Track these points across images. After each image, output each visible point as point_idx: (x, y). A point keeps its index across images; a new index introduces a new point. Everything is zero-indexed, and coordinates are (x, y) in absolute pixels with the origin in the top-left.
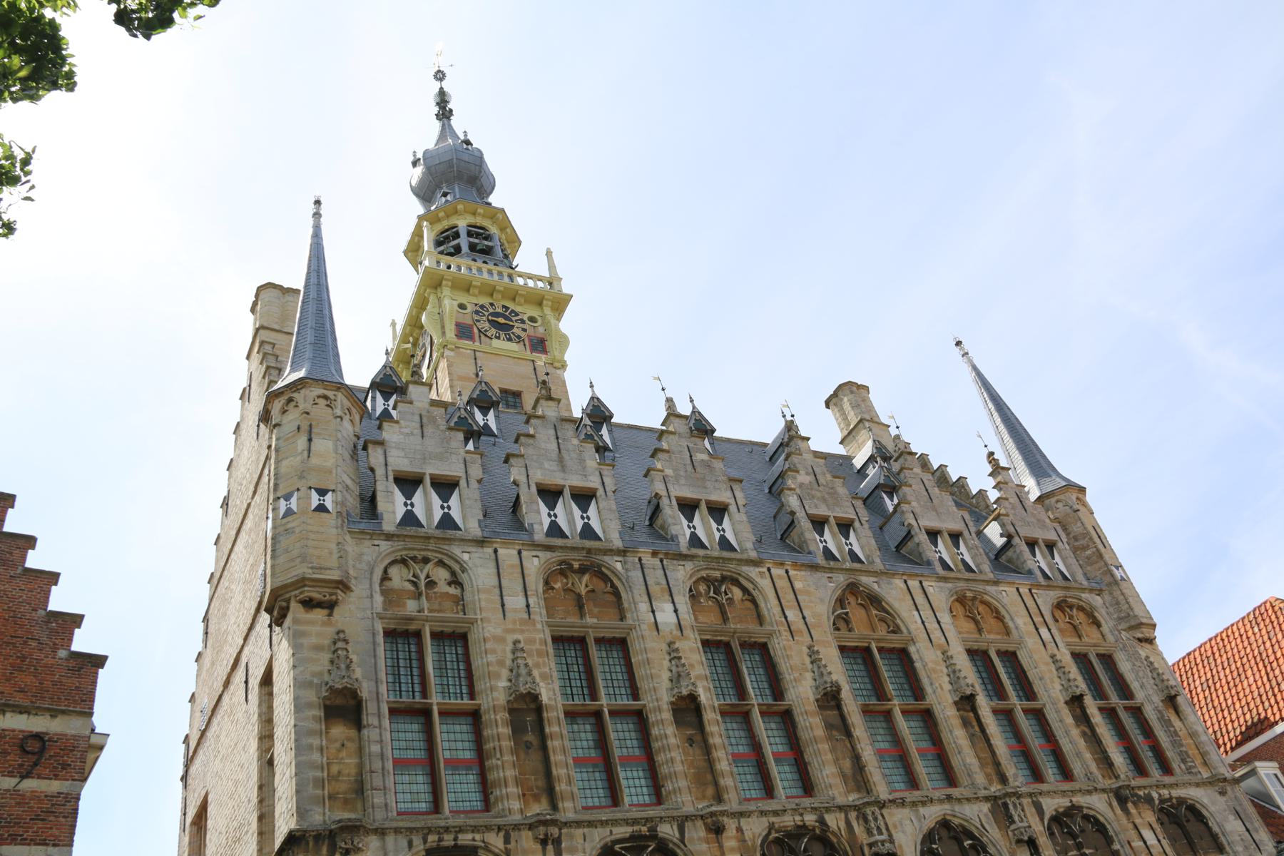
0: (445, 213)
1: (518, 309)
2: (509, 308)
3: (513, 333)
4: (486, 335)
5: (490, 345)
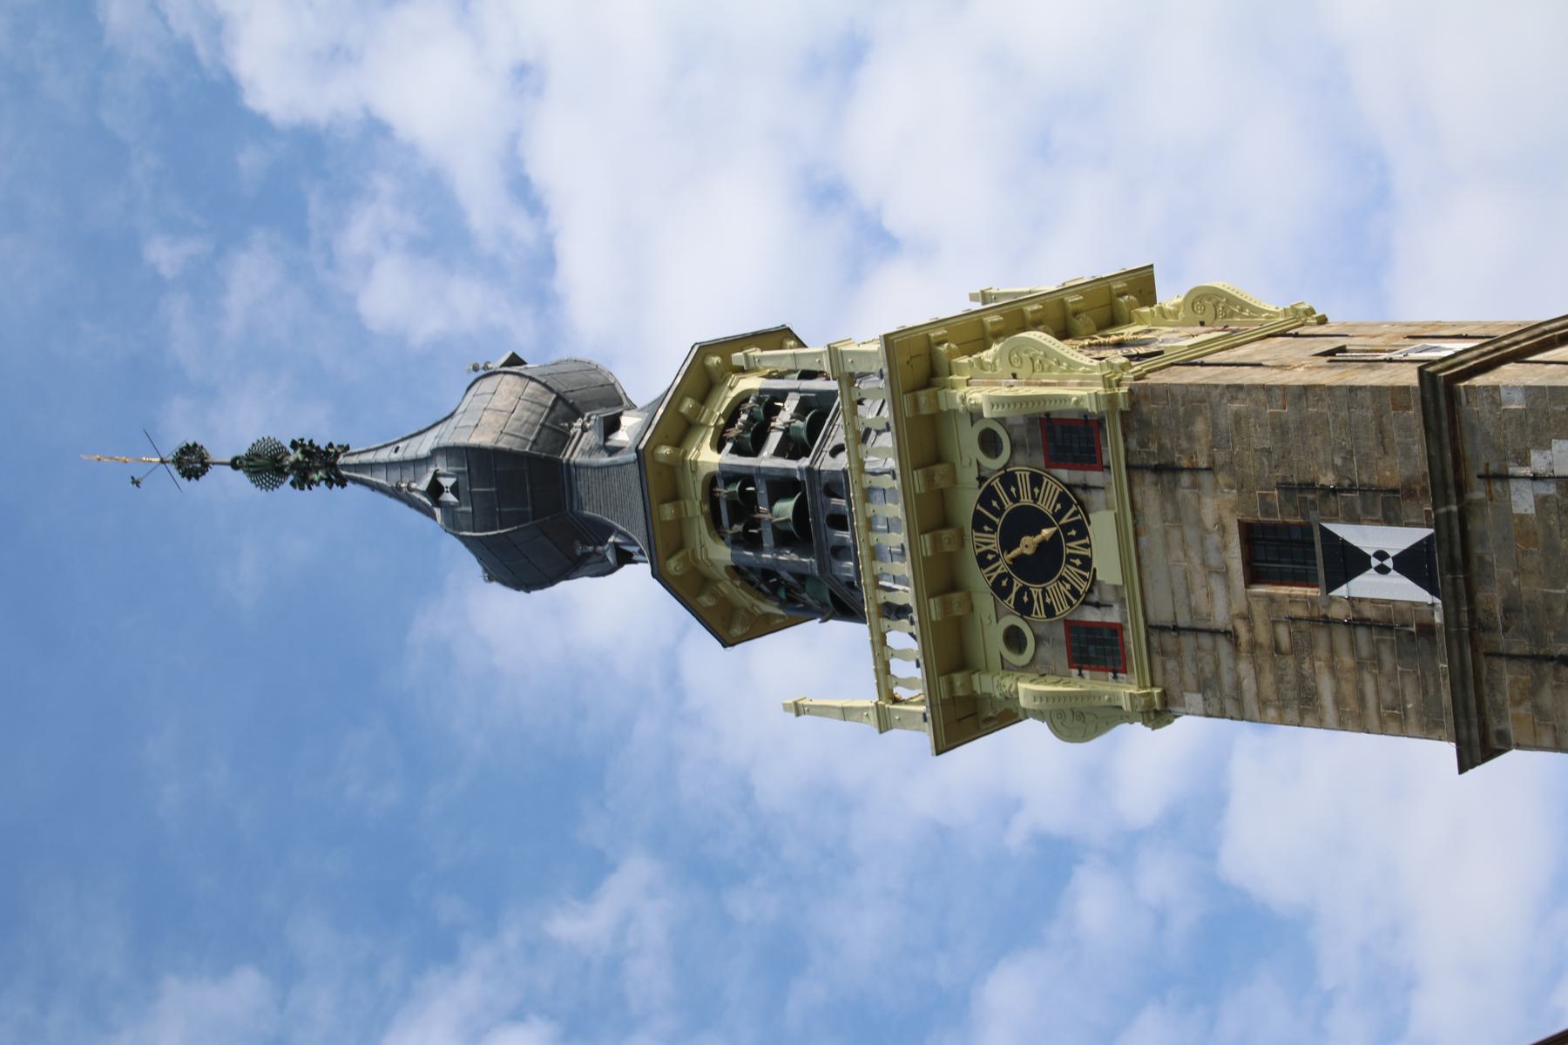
0: (699, 594)
1: (969, 476)
2: (977, 513)
4: (1090, 591)
5: (1116, 587)
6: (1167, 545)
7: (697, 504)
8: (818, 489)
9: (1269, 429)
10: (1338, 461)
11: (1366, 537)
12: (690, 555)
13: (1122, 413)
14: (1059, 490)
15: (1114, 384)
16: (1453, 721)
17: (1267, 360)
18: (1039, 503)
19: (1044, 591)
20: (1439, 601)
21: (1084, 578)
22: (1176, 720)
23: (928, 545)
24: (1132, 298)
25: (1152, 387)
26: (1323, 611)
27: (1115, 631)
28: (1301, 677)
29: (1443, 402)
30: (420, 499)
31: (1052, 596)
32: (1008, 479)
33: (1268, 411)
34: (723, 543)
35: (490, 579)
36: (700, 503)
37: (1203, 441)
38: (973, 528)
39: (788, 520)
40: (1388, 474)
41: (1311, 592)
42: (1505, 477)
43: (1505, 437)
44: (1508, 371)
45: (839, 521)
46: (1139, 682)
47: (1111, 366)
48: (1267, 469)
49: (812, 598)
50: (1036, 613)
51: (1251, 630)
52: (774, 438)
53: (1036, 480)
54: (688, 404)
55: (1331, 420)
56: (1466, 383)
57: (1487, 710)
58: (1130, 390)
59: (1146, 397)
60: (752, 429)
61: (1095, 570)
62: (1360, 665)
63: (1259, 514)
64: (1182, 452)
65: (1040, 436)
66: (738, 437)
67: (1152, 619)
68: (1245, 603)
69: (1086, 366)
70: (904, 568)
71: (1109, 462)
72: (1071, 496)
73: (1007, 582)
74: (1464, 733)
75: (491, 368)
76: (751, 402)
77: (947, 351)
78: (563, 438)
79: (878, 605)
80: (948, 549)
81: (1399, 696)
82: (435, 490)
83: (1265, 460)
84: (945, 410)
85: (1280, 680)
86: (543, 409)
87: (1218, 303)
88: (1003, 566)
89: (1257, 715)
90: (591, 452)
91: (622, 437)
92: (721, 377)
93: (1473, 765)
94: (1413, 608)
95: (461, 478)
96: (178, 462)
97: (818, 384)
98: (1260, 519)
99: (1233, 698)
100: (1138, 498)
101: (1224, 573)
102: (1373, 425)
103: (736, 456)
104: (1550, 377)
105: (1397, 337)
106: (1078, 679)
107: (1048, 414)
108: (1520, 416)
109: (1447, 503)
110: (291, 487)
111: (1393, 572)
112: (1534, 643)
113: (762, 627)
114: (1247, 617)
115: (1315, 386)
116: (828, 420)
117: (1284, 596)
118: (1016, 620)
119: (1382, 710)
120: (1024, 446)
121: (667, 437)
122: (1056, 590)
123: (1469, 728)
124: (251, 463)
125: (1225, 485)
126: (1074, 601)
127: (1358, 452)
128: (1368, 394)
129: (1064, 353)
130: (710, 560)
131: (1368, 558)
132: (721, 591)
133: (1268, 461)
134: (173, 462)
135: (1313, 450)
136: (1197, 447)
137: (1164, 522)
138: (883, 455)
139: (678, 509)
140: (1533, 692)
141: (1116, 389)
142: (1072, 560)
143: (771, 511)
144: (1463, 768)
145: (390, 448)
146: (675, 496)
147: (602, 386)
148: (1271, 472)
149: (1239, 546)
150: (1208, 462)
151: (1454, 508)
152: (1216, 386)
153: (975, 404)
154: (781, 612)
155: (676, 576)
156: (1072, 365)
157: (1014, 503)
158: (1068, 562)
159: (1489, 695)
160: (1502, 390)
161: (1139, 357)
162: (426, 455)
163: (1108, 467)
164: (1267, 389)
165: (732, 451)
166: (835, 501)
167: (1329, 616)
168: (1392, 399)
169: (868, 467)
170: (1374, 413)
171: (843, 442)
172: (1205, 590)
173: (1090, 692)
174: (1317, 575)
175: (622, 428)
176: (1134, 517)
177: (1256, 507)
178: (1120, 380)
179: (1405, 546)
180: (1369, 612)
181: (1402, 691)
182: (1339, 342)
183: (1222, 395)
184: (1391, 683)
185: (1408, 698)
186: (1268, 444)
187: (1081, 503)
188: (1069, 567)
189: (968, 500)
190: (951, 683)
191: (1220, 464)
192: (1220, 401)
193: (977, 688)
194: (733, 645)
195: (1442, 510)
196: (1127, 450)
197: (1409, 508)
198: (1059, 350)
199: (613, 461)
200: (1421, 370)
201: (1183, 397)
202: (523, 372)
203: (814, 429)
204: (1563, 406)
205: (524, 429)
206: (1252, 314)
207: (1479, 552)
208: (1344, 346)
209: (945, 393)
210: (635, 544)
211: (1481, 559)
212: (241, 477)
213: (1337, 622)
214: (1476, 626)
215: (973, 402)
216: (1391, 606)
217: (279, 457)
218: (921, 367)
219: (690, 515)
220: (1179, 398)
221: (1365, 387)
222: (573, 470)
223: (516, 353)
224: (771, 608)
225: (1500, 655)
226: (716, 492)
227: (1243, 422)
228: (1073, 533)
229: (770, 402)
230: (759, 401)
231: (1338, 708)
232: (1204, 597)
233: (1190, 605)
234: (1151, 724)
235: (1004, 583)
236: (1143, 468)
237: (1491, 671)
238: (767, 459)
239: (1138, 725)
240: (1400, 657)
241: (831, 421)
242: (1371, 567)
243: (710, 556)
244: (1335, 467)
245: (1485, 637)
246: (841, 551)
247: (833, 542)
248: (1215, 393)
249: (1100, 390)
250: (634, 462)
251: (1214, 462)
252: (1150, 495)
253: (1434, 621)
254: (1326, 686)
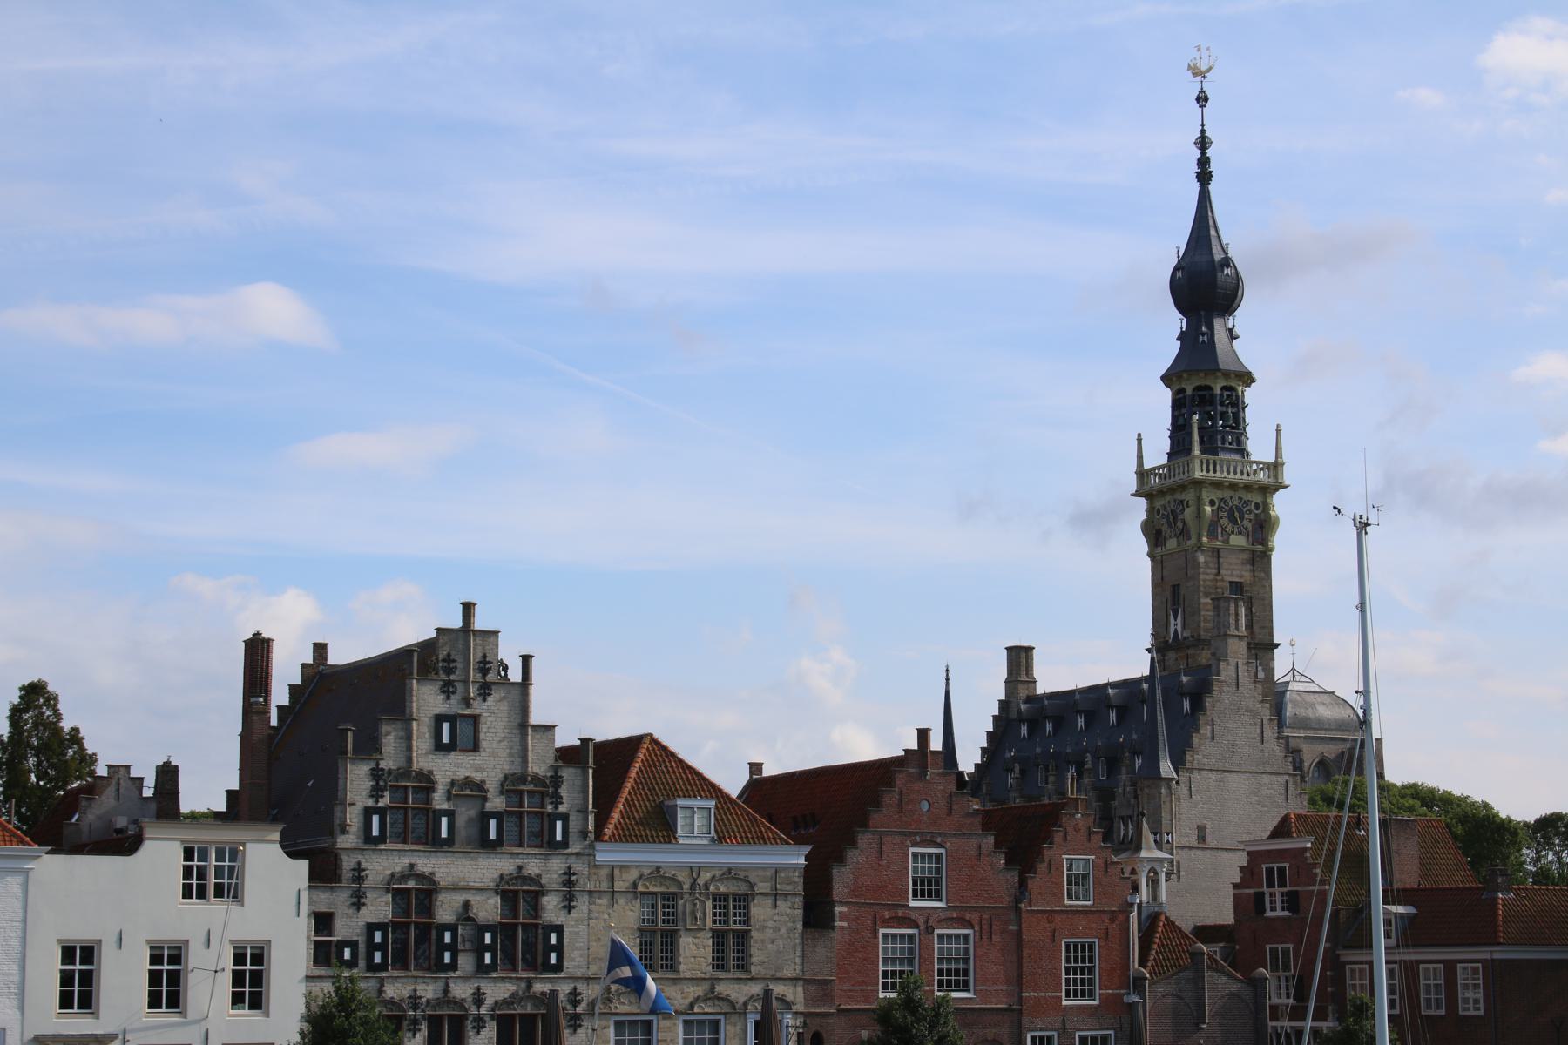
53: (1250, 520)
101: (1232, 575)
122: (1224, 522)
163: (1253, 545)
252: (1246, 556)
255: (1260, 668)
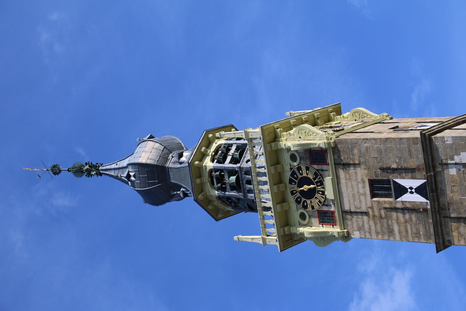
0: (208, 205)
1: (287, 168)
2: (290, 179)
3: (314, 179)
5: (332, 200)
6: (347, 187)
7: (207, 178)
8: (243, 173)
9: (376, 151)
10: (397, 160)
11: (406, 183)
12: (205, 193)
13: (333, 148)
14: (314, 171)
15: (330, 139)
16: (434, 237)
17: (375, 131)
18: (309, 175)
19: (311, 202)
20: (429, 201)
21: (323, 197)
22: (352, 239)
23: (276, 188)
24: (335, 113)
25: (341, 140)
26: (394, 205)
27: (333, 213)
28: (388, 225)
29: (428, 142)
30: (124, 179)
31: (313, 203)
32: (299, 168)
33: (376, 146)
34: (215, 190)
35: (146, 202)
36: (208, 178)
37: (357, 156)
38: (289, 183)
39: (234, 183)
40: (412, 164)
41: (391, 200)
42: (447, 164)
43: (447, 152)
44: (447, 132)
45: (249, 182)
46: (340, 228)
47: (329, 134)
48: (376, 163)
49: (242, 206)
50: (309, 208)
51: (373, 212)
52: (229, 158)
53: (307, 169)
54: (203, 148)
55: (394, 148)
56: (434, 136)
57: (444, 233)
58: (334, 141)
59: (339, 143)
60: (222, 155)
61: (326, 195)
62: (406, 222)
63: (374, 177)
64: (350, 159)
65: (308, 155)
66: (218, 158)
67: (343, 210)
68: (371, 203)
69: (321, 134)
70: (269, 196)
71: (329, 163)
72: (318, 173)
73: (300, 200)
74: (438, 241)
75: (144, 140)
76: (222, 147)
77: (280, 131)
78: (166, 160)
79: (261, 207)
80: (282, 190)
81: (418, 230)
82: (128, 176)
83: (375, 161)
84: (280, 148)
85: (382, 226)
86: (160, 151)
87: (361, 113)
88: (298, 194)
89: (375, 237)
90: (174, 163)
91: (183, 159)
92: (213, 140)
93: (441, 250)
94: (421, 204)
95: (136, 172)
96: (52, 170)
97: (242, 142)
98: (375, 178)
99: (368, 232)
100: (338, 173)
101: (365, 195)
102: (407, 149)
103: (218, 164)
104: (459, 134)
105: (413, 123)
106: (322, 228)
107: (310, 149)
108: (451, 145)
109: (430, 172)
110: (86, 177)
111: (415, 193)
112: (458, 213)
113: (227, 215)
114: (372, 208)
115: (389, 138)
116: (245, 152)
117: (383, 201)
118: (303, 211)
119: (413, 235)
120: (303, 158)
121: (197, 159)
122: (315, 202)
123: (439, 239)
124: (73, 170)
125: (364, 168)
126: (320, 204)
127: (403, 158)
128: (405, 140)
129: (314, 130)
130: (211, 195)
131: (407, 189)
132: (215, 204)
133: (376, 161)
134: (50, 170)
135: (390, 157)
136: (355, 157)
137: (346, 180)
138: (262, 161)
139: (201, 180)
140: (458, 228)
141: (330, 140)
142: (319, 192)
143: (229, 180)
144: (438, 252)
145: (115, 164)
146: (200, 176)
147: (178, 144)
148: (377, 164)
149: (369, 187)
150: (359, 162)
151: (432, 173)
152: (360, 139)
153: (288, 146)
154: (233, 210)
155: (201, 200)
156: (317, 134)
157: (301, 176)
158: (318, 193)
159: (445, 229)
160: (445, 138)
161: (337, 131)
162: (125, 166)
163: (329, 164)
164: (375, 139)
165: (217, 162)
166: (248, 176)
167: (396, 207)
168: (413, 141)
169: (257, 166)
170: (407, 145)
171: (250, 159)
172: (359, 200)
173: (325, 231)
174: (392, 194)
175: (184, 156)
176: (337, 179)
177: (373, 175)
178: (331, 138)
179: (418, 185)
180: (408, 205)
181: (419, 229)
182: (396, 125)
183: (362, 142)
184: (415, 226)
185: (420, 231)
186: (376, 156)
187: (321, 175)
188: (318, 194)
189: (288, 175)
190: (284, 230)
191: (362, 162)
192: (361, 144)
193: (292, 231)
194: (219, 220)
195: (429, 174)
196: (334, 159)
197: (417, 174)
198: (313, 129)
199: (181, 166)
200: (421, 132)
201: (350, 142)
202: (153, 140)
203: (241, 155)
204: (463, 142)
205: (154, 158)
206: (370, 117)
207: (440, 186)
208: (398, 126)
209: (280, 143)
210: (189, 191)
211: (441, 188)
212: (71, 173)
213: (398, 209)
214: (440, 209)
215: (288, 146)
216: (414, 203)
217: (82, 168)
218: (272, 136)
219: (205, 182)
220: (349, 143)
221: (404, 138)
222: (170, 169)
223: (152, 135)
224: (230, 209)
225: (447, 217)
226: (212, 175)
227: (368, 149)
228: (319, 184)
229: (228, 147)
230: (224, 147)
231: (400, 235)
232: (358, 202)
233: (355, 205)
234: (344, 241)
235: (299, 200)
236: (340, 164)
237: (445, 222)
238: (227, 164)
239: (340, 241)
240: (418, 218)
241: (246, 153)
242: (408, 192)
243: (211, 194)
244: (396, 162)
245: (443, 212)
246: (250, 191)
247: (247, 189)
248: (360, 141)
249: (326, 141)
250: (188, 166)
251: (360, 162)
252: (342, 173)
253: (427, 207)
254: (396, 228)
255: (457, 159)
